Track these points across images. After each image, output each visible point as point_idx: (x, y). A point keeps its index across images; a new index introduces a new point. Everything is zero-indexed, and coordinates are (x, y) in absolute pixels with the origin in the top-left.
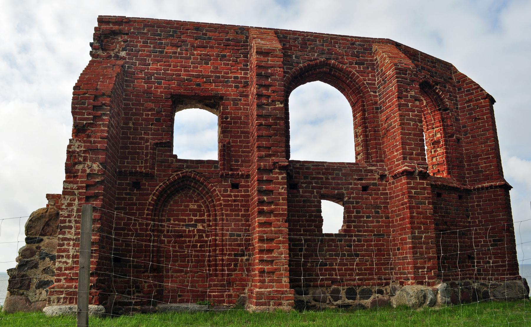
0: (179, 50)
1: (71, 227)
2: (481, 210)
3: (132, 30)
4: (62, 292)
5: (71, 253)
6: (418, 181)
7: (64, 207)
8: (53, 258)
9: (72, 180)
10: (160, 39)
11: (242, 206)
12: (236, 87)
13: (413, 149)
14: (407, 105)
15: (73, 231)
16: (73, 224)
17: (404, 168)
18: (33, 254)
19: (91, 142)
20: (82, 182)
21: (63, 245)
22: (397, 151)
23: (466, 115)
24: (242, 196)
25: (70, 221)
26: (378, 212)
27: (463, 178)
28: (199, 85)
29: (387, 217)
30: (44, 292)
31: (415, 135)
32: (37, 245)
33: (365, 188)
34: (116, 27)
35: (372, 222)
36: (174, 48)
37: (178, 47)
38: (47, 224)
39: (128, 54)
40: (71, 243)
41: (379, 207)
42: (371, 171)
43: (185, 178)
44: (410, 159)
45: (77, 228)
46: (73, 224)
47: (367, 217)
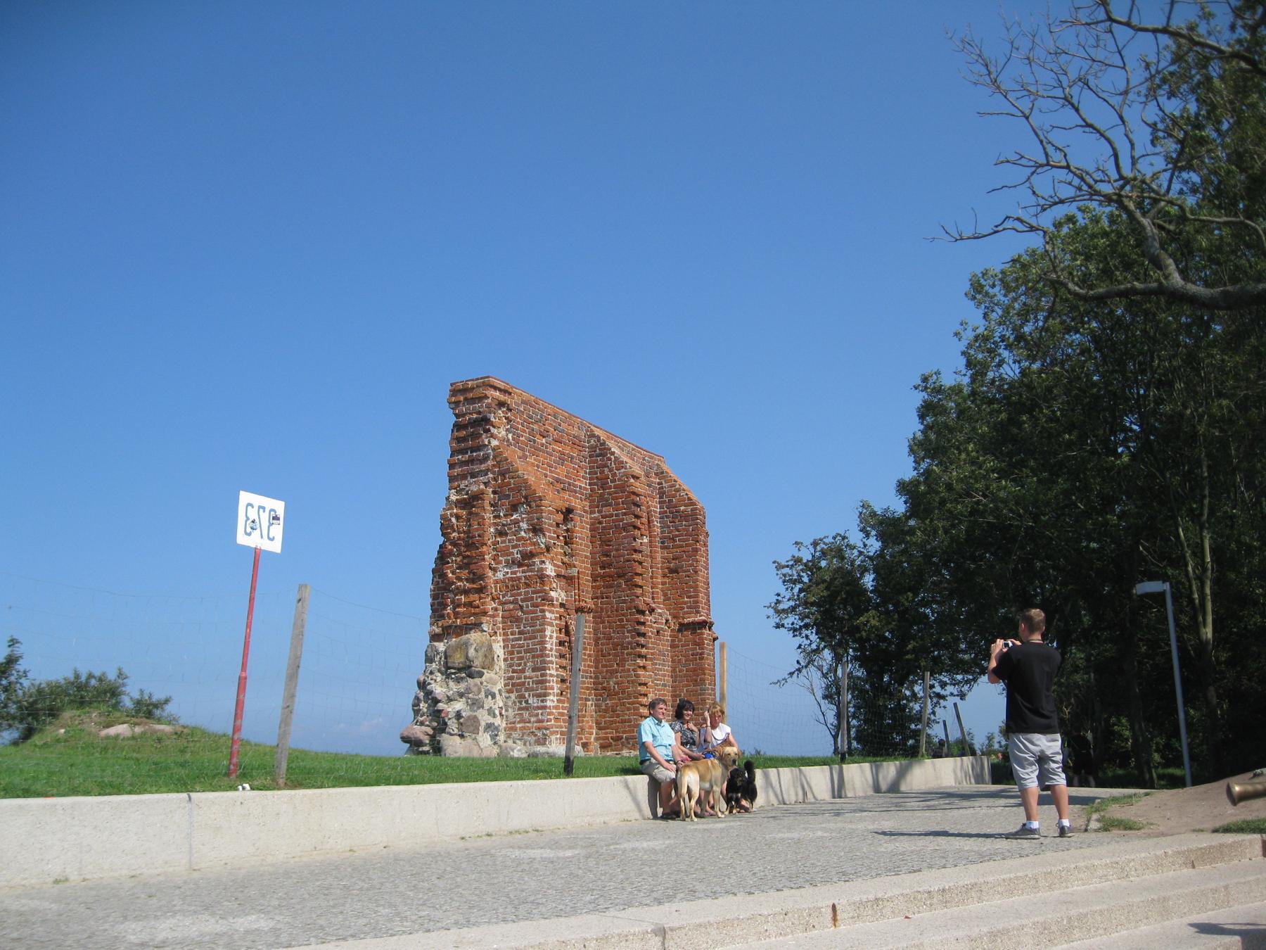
0: (544, 441)
4: (557, 732)
7: (547, 639)
8: (494, 696)
11: (589, 644)
12: (581, 499)
16: (554, 659)
21: (549, 682)
22: (688, 597)
24: (589, 633)
30: (488, 736)
33: (658, 632)
34: (502, 397)
37: (544, 437)
39: (513, 439)
40: (555, 679)
46: (554, 659)
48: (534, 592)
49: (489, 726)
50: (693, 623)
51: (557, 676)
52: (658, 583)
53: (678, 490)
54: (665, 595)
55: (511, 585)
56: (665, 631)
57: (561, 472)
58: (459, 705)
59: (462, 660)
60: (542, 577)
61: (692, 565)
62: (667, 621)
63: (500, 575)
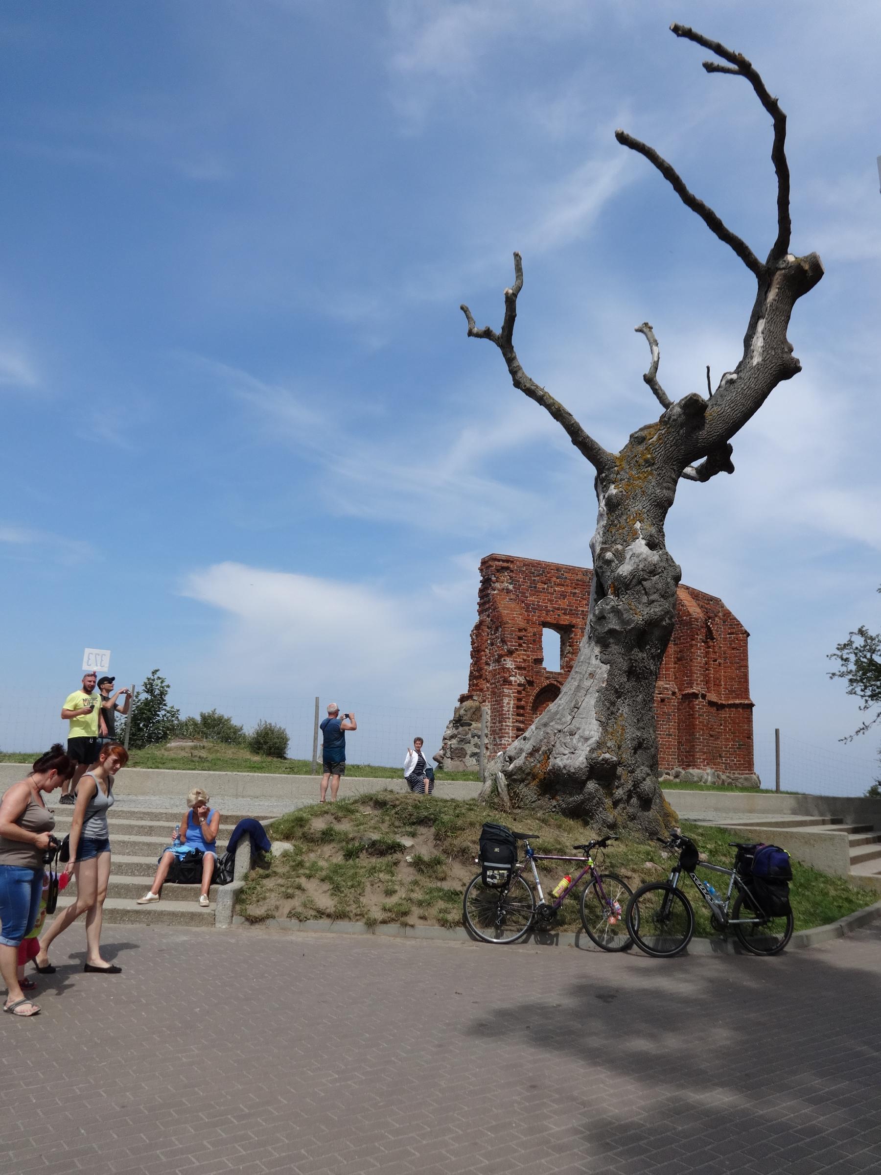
0: (546, 586)
1: (509, 718)
2: (731, 720)
3: (516, 568)
5: (511, 735)
6: (701, 700)
7: (505, 705)
8: (479, 737)
9: (507, 686)
10: (534, 576)
13: (698, 677)
14: (697, 645)
15: (511, 720)
16: (510, 716)
17: (693, 691)
18: (467, 734)
19: (516, 662)
20: (515, 689)
21: (506, 729)
23: (727, 644)
25: (509, 714)
26: (669, 718)
27: (720, 694)
28: (559, 615)
29: (675, 722)
30: (474, 760)
31: (700, 667)
32: (469, 727)
33: (663, 700)
34: (505, 565)
35: (665, 725)
36: (543, 584)
37: (545, 584)
38: (474, 713)
39: (514, 588)
40: (511, 728)
41: (671, 715)
42: (667, 688)
43: (551, 685)
44: (697, 684)
45: (513, 719)
47: (663, 721)
48: (501, 678)
49: (474, 755)
50: (688, 694)
51: (513, 726)
52: (671, 668)
53: (682, 605)
54: (675, 675)
55: (494, 673)
56: (673, 699)
57: (564, 603)
58: (454, 741)
59: (458, 716)
60: (504, 669)
61: (688, 656)
62: (674, 693)
63: (491, 668)
